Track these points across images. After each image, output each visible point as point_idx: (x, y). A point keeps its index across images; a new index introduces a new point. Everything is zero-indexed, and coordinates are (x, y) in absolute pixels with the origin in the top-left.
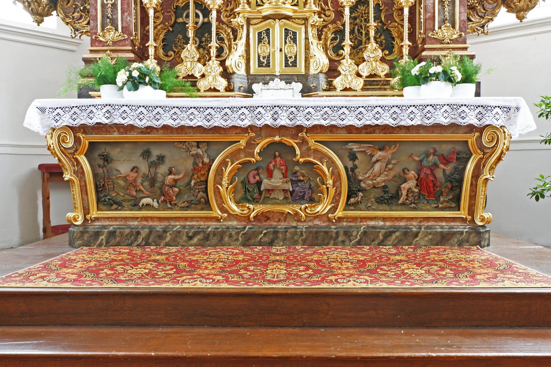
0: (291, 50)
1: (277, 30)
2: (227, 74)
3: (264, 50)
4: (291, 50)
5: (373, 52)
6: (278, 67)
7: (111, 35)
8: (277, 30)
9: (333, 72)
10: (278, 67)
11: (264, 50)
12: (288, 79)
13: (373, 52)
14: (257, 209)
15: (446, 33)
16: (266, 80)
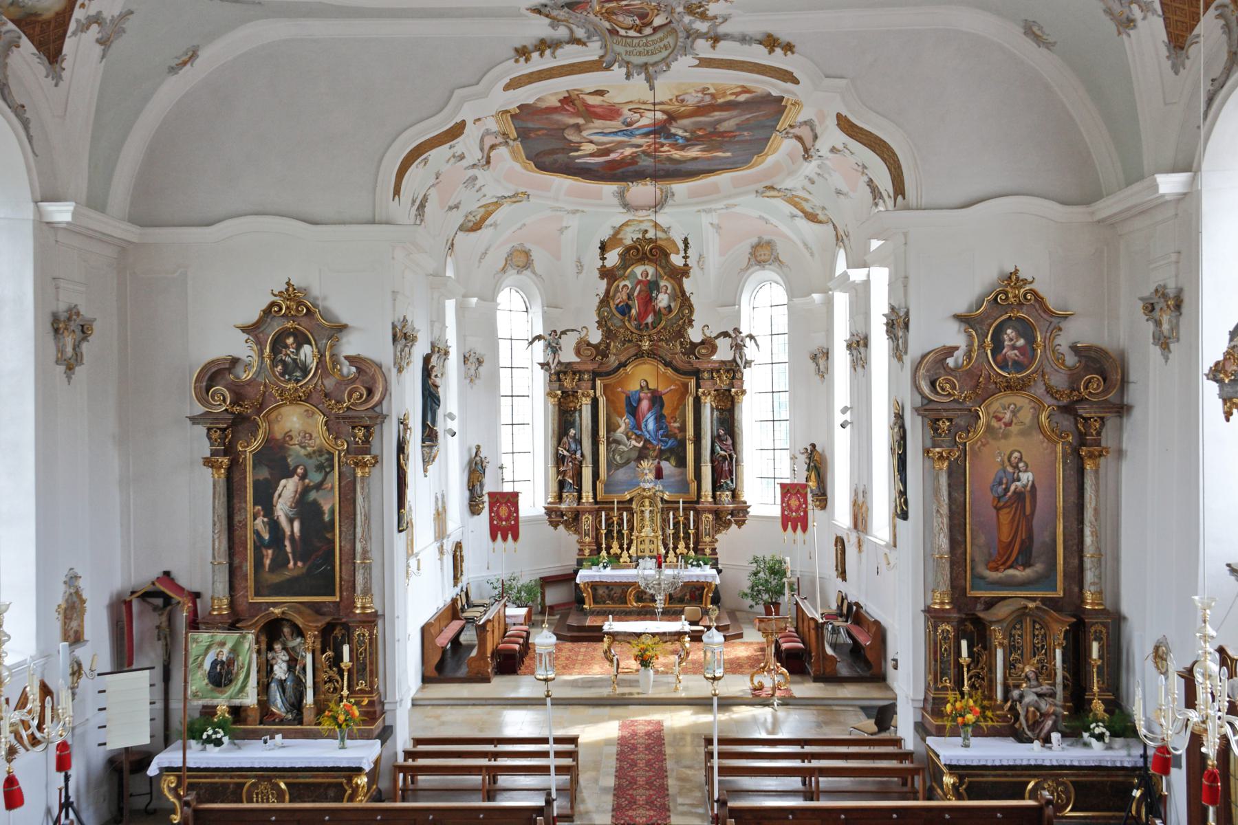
0: (652, 547)
1: (647, 541)
2: (630, 557)
3: (642, 547)
4: (652, 547)
5: (682, 545)
6: (647, 553)
7: (587, 540)
8: (647, 541)
9: (666, 556)
10: (647, 553)
11: (642, 547)
12: (651, 557)
13: (682, 545)
14: (641, 605)
15: (707, 539)
16: (643, 558)
